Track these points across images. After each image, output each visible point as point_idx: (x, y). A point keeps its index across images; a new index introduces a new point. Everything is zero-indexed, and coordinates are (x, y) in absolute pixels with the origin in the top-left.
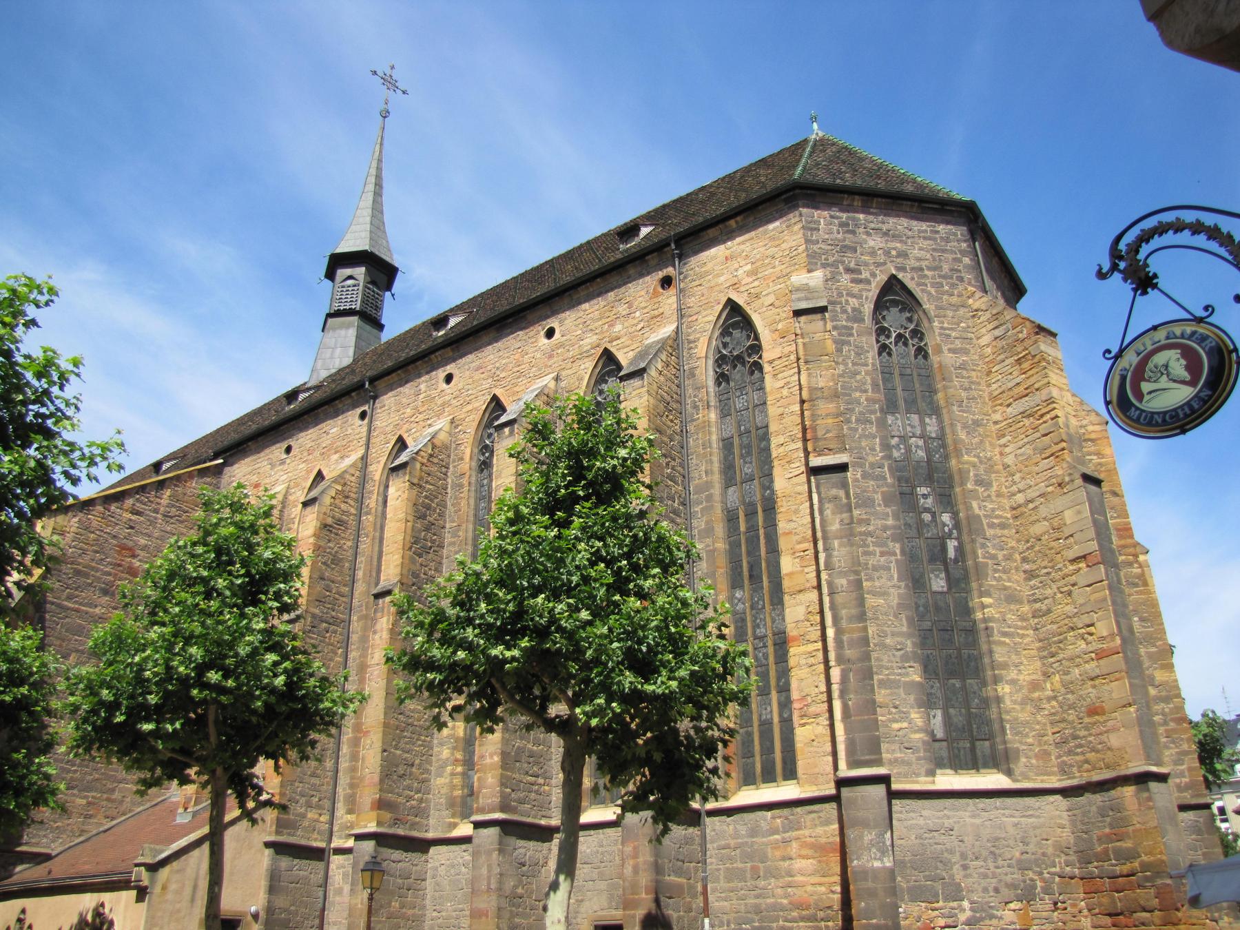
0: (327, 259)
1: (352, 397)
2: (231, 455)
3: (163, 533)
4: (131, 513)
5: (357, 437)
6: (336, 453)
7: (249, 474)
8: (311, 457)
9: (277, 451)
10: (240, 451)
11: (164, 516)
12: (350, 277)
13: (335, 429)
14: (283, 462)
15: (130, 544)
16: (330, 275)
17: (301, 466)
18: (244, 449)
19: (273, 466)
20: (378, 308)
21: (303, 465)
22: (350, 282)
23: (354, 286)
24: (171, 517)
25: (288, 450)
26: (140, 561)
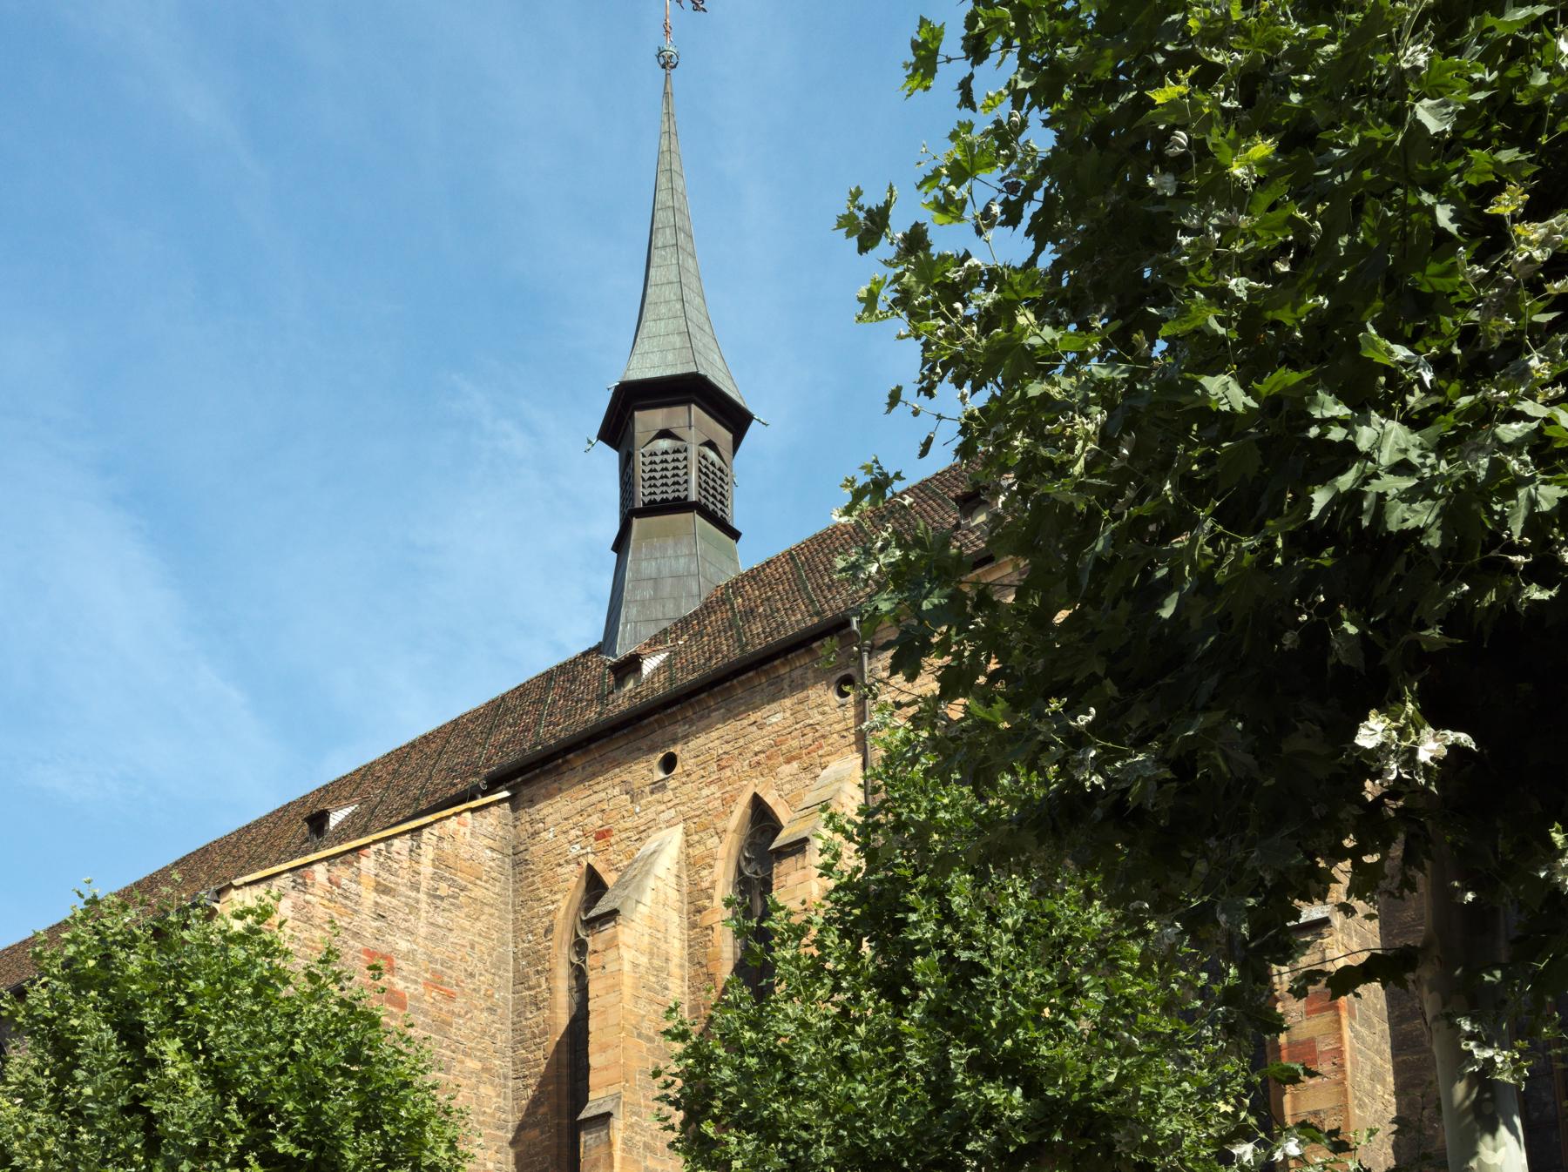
0: (609, 395)
1: (811, 651)
2: (525, 783)
3: (432, 929)
4: (376, 890)
5: (838, 727)
6: (788, 762)
7: (580, 813)
8: (728, 772)
9: (647, 769)
10: (549, 772)
11: (430, 895)
12: (665, 434)
13: (779, 716)
14: (659, 787)
15: (384, 949)
16: (616, 431)
17: (706, 792)
18: (558, 766)
19: (634, 796)
20: (723, 499)
21: (713, 788)
22: (664, 444)
23: (677, 451)
24: (442, 898)
25: (669, 763)
26: (404, 978)
